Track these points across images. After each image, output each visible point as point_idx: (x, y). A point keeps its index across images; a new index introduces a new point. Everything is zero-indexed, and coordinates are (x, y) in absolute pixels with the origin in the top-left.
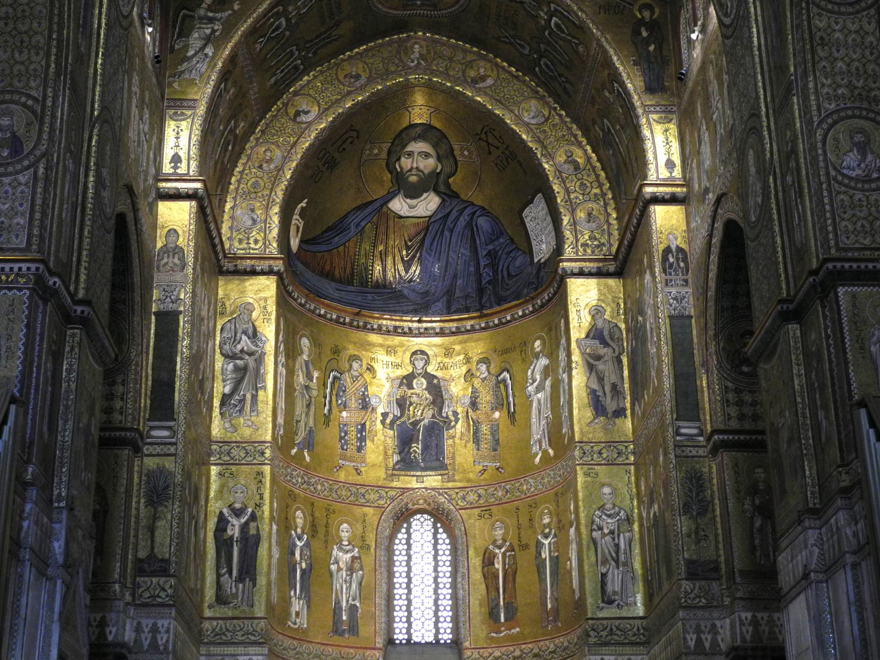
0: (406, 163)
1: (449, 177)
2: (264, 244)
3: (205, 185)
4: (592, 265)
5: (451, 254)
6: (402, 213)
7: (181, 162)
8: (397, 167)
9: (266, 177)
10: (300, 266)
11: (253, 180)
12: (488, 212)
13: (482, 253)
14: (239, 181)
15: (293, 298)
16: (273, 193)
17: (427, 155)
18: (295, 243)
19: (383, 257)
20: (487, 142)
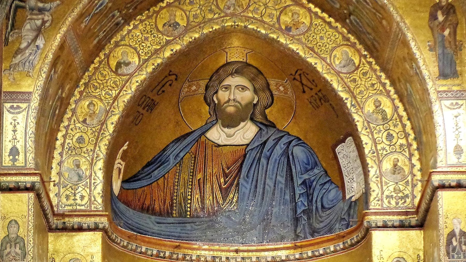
0: (223, 95)
1: (266, 108)
2: (90, 199)
3: (42, 179)
4: (396, 218)
5: (268, 181)
6: (220, 142)
7: (18, 154)
8: (215, 99)
9: (90, 132)
10: (122, 206)
11: (78, 135)
12: (304, 143)
13: (298, 181)
14: (64, 137)
15: (116, 243)
16: (97, 148)
17: (244, 88)
18: (117, 187)
19: (202, 186)
20: (301, 82)
